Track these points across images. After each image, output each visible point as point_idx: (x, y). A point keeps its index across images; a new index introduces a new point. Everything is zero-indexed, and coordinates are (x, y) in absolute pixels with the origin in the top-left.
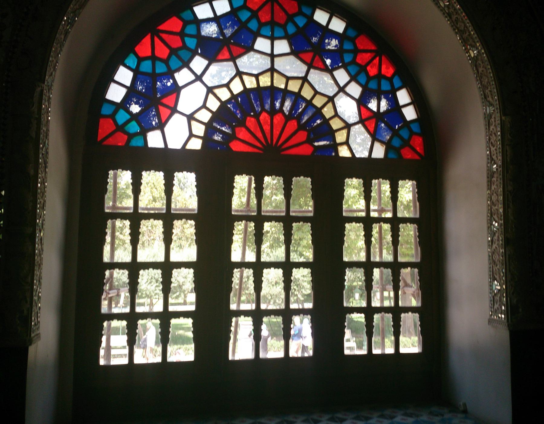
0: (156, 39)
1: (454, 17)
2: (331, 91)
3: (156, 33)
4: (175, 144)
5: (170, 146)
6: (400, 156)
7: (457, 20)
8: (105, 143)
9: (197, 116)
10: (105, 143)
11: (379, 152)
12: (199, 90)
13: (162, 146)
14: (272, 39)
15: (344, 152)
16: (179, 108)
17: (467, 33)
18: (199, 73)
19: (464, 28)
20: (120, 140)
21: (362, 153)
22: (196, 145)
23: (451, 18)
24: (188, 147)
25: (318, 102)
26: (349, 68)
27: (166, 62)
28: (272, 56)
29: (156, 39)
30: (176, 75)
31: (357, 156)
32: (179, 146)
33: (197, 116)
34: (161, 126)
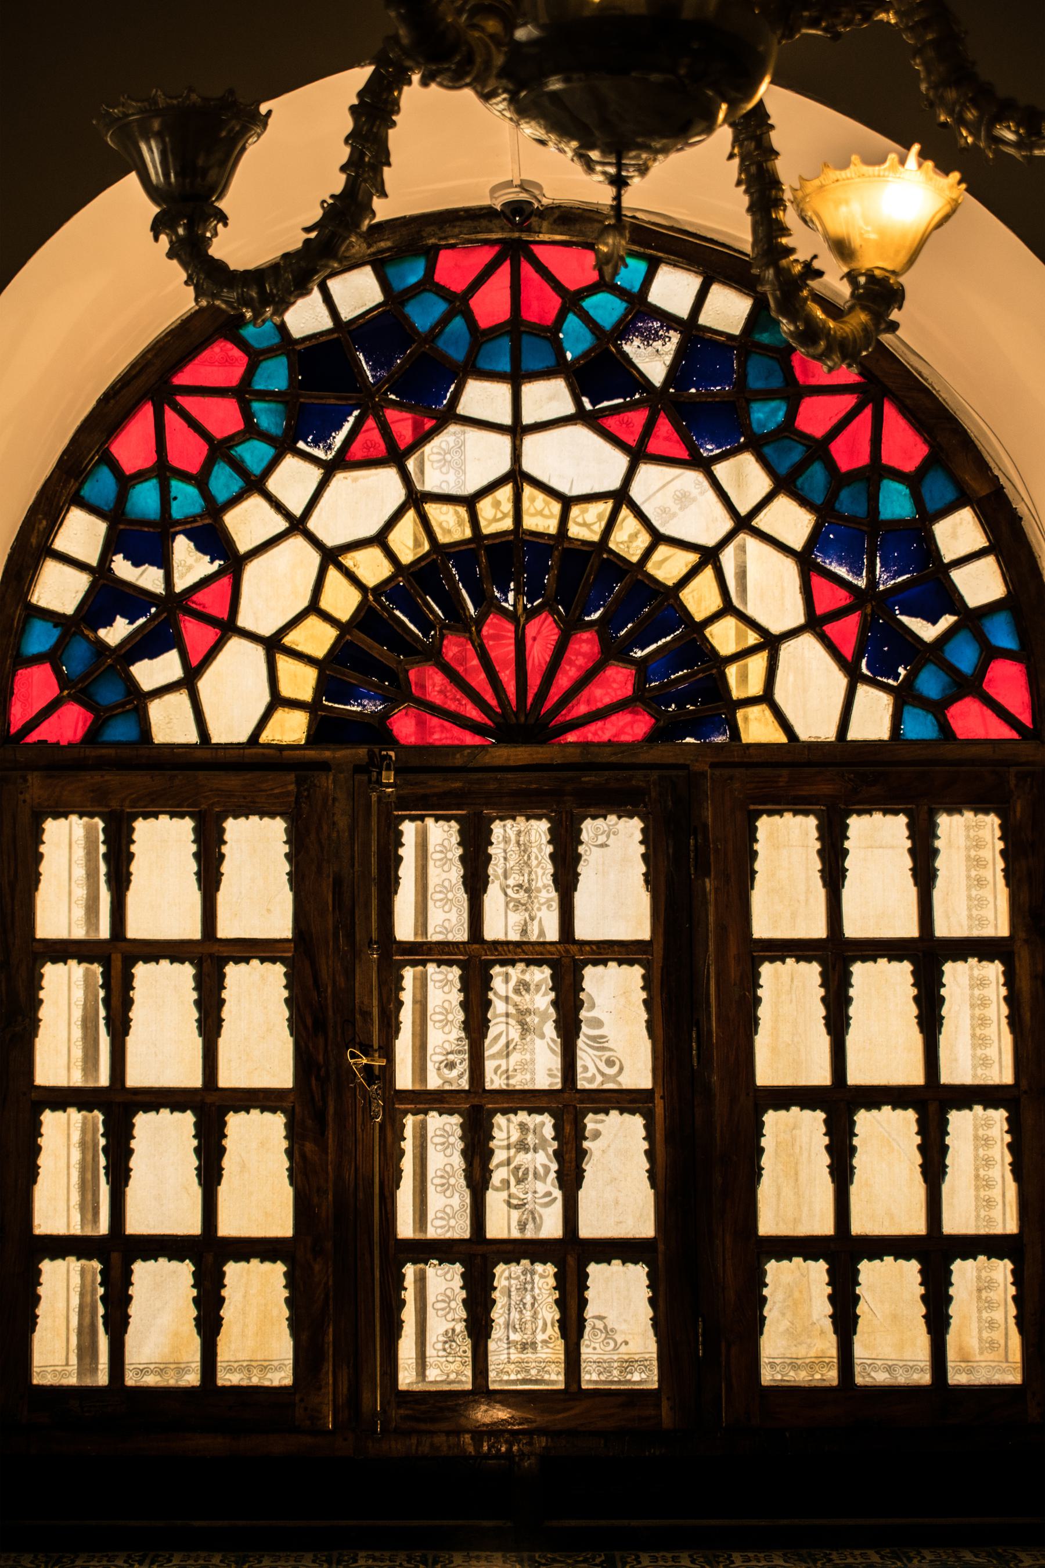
0: (170, 415)
5: (217, 736)
6: (945, 729)
9: (290, 639)
10: (34, 737)
13: (192, 737)
14: (516, 378)
16: (244, 620)
24: (269, 735)
26: (767, 450)
27: (201, 481)
29: (170, 415)
30: (231, 519)
33: (290, 639)
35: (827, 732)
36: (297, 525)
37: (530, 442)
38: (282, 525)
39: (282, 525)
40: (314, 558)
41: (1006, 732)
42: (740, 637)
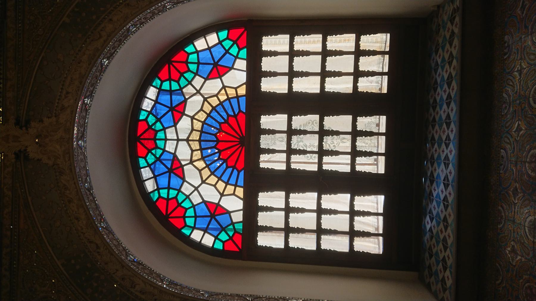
1: (143, 20)
2: (199, 99)
3: (167, 216)
4: (239, 204)
7: (145, 18)
8: (240, 247)
11: (241, 64)
13: (242, 212)
15: (242, 91)
17: (155, 11)
18: (194, 189)
19: (151, 13)
20: (239, 240)
22: (240, 192)
23: (144, 22)
24: (241, 195)
25: (207, 108)
28: (178, 140)
31: (244, 80)
32: (241, 202)
34: (229, 213)
40: (204, 185)
41: (246, 33)
42: (223, 95)
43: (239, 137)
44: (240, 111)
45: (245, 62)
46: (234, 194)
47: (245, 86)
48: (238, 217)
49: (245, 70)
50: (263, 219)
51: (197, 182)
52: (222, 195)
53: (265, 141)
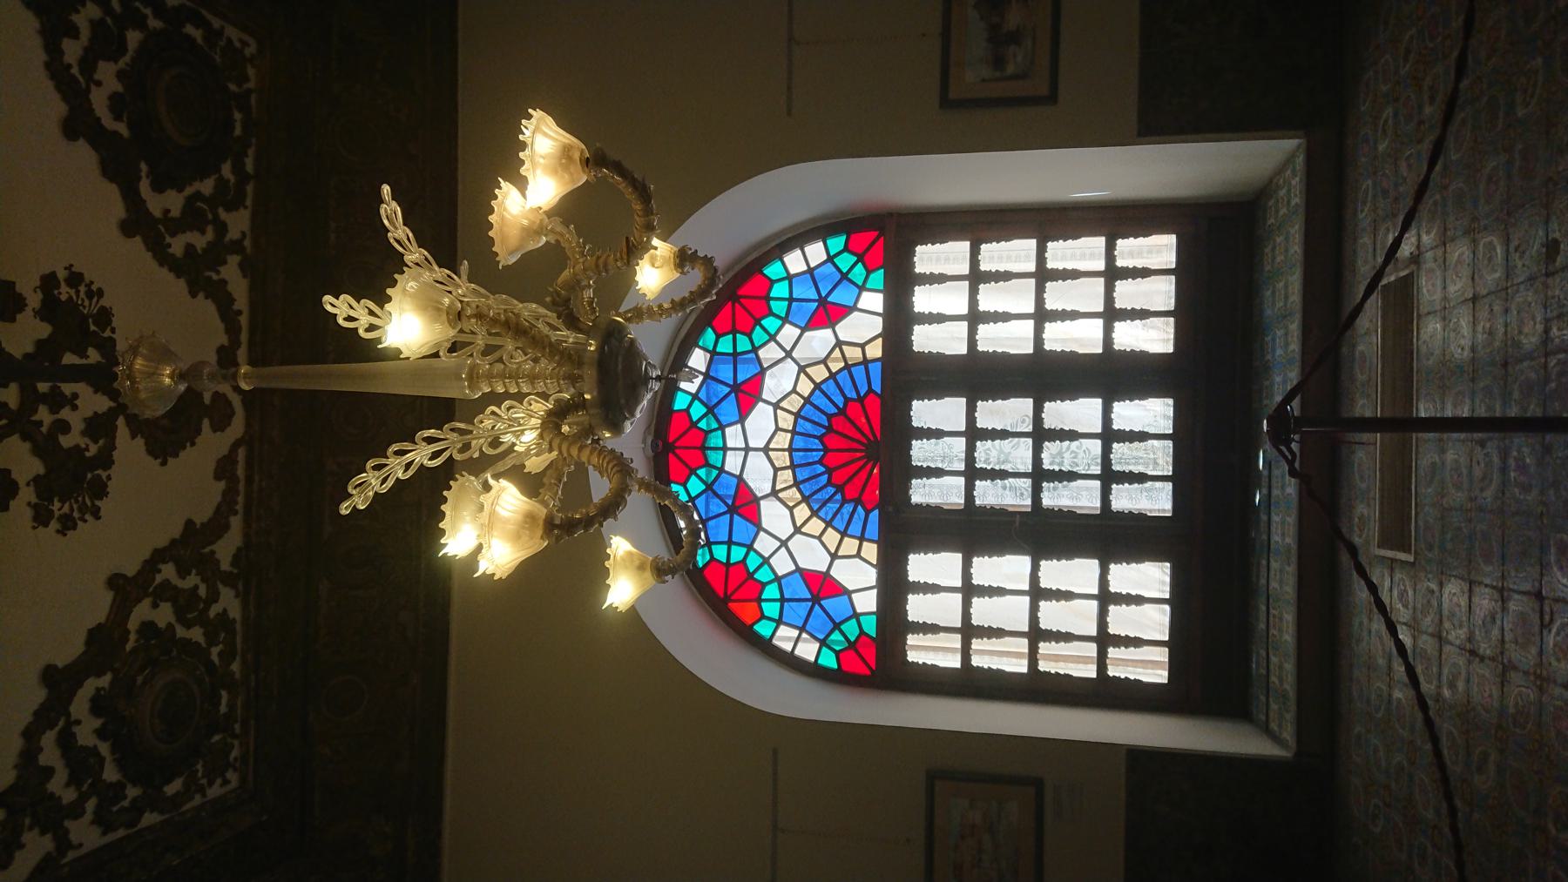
4: (870, 576)
8: (874, 667)
10: (874, 667)
11: (874, 301)
12: (797, 543)
13: (875, 591)
15: (875, 351)
21: (877, 325)
22: (871, 551)
31: (879, 329)
35: (879, 320)
36: (784, 543)
37: (752, 445)
38: (783, 549)
39: (783, 549)
43: (866, 442)
44: (870, 391)
45: (880, 297)
46: (858, 555)
47: (880, 341)
48: (867, 602)
49: (880, 309)
50: (917, 608)
51: (785, 529)
52: (834, 556)
53: (921, 451)
